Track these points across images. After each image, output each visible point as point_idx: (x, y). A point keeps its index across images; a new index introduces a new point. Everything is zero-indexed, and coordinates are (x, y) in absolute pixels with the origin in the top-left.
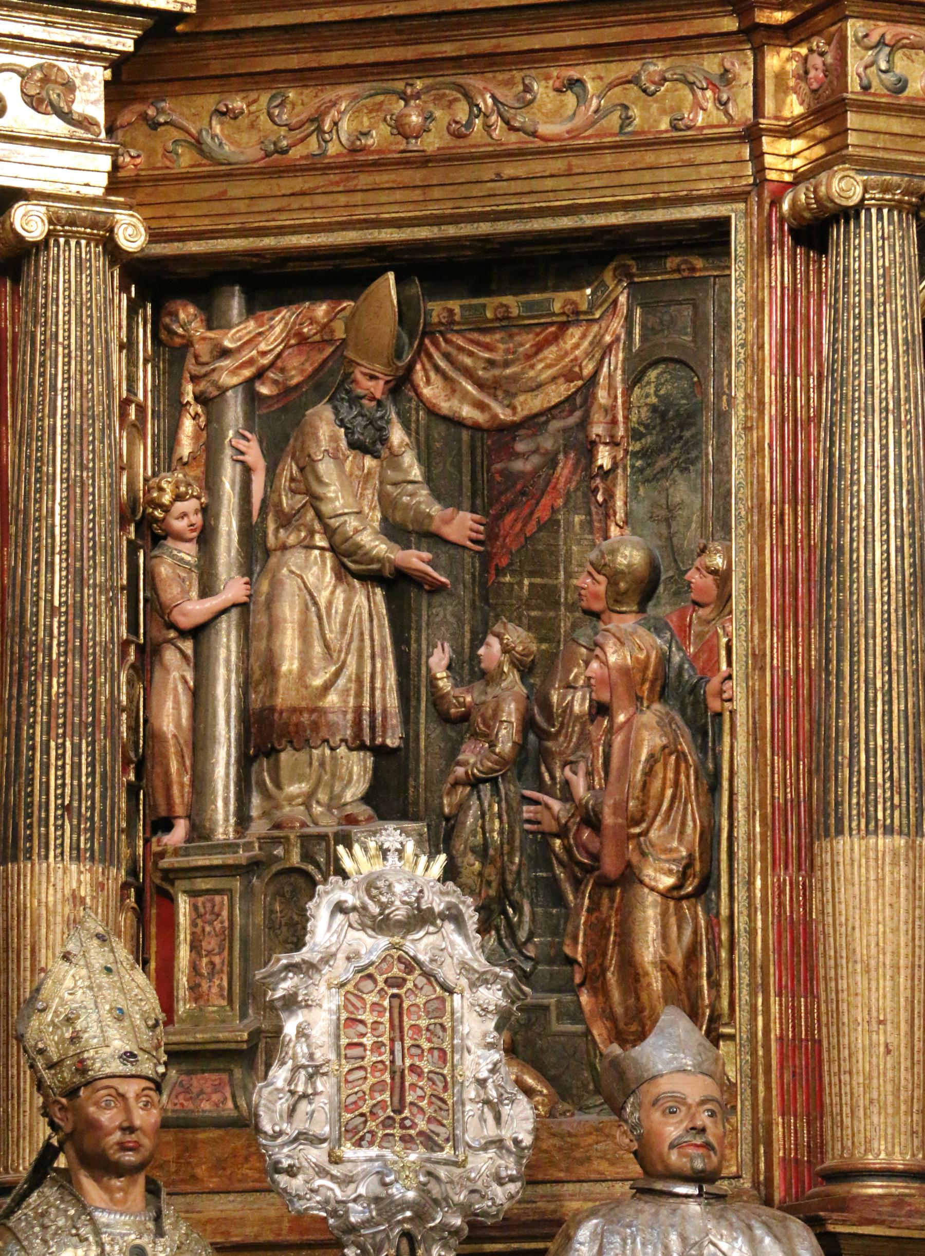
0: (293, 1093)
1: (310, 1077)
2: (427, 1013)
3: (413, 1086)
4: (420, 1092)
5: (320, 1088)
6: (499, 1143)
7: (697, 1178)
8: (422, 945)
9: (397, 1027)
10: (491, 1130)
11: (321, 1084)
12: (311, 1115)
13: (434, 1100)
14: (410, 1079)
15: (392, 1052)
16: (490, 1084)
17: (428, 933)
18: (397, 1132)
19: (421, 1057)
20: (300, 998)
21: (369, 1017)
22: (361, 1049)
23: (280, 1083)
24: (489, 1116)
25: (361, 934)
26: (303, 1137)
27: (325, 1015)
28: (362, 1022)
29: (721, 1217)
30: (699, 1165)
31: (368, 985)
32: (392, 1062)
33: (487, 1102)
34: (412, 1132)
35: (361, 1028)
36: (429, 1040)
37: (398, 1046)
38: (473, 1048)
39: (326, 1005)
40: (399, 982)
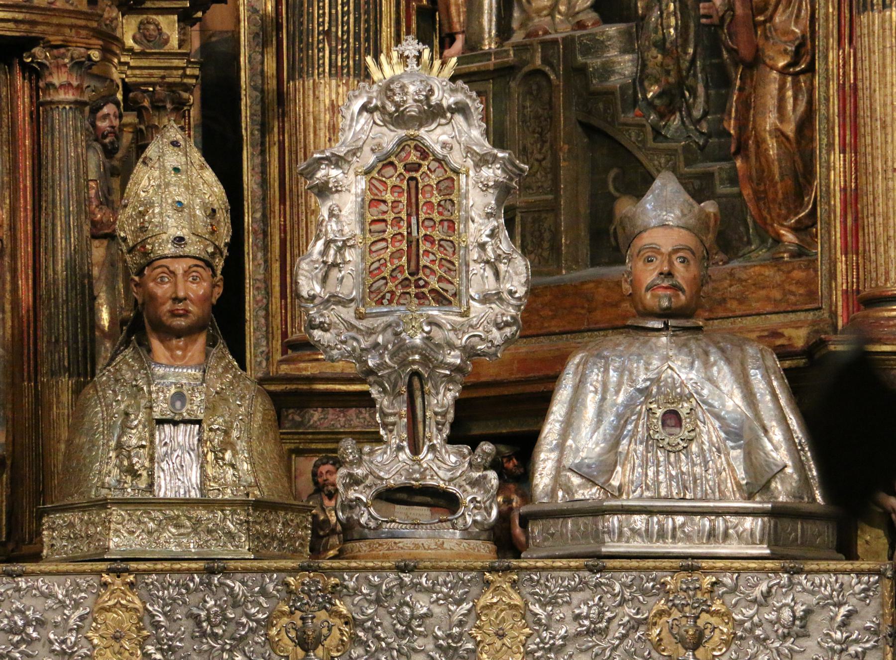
0: (324, 263)
1: (340, 250)
2: (439, 191)
3: (426, 252)
4: (432, 257)
5: (348, 258)
6: (498, 297)
7: (665, 314)
8: (433, 136)
9: (413, 207)
10: (491, 284)
11: (350, 255)
12: (341, 281)
13: (444, 262)
14: (424, 246)
15: (409, 225)
16: (489, 249)
17: (439, 125)
18: (413, 290)
19: (433, 227)
20: (330, 186)
21: (389, 197)
22: (383, 224)
23: (315, 256)
24: (489, 273)
25: (384, 129)
26: (335, 300)
27: (353, 198)
28: (384, 202)
29: (685, 345)
30: (665, 303)
31: (389, 171)
32: (409, 234)
33: (487, 262)
34: (425, 290)
35: (383, 207)
36: (440, 213)
37: (413, 220)
38: (477, 219)
39: (353, 191)
40: (417, 167)
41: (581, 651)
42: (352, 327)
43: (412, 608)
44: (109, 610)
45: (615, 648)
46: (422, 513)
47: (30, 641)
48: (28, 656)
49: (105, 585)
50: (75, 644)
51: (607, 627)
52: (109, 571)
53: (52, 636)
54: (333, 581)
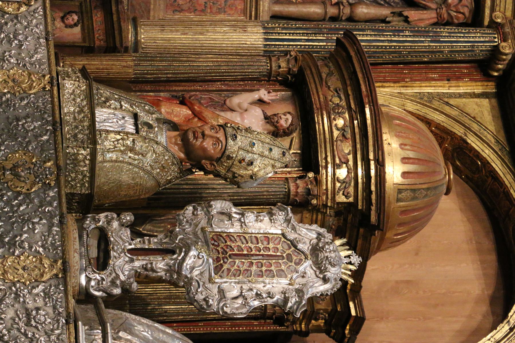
17: (315, 271)
20: (274, 217)
22: (256, 243)
28: (269, 244)
41: (16, 311)
42: (196, 226)
43: (38, 223)
44: (29, 78)
45: (19, 330)
46: (94, 253)
47: (10, 42)
48: (2, 42)
49: (44, 76)
50: (10, 62)
51: (31, 325)
52: (52, 78)
53: (13, 52)
54: (53, 183)
